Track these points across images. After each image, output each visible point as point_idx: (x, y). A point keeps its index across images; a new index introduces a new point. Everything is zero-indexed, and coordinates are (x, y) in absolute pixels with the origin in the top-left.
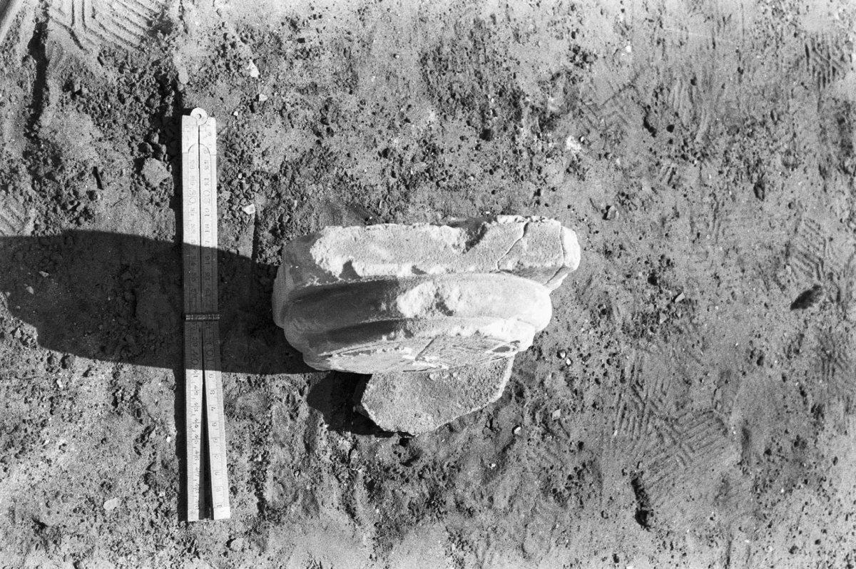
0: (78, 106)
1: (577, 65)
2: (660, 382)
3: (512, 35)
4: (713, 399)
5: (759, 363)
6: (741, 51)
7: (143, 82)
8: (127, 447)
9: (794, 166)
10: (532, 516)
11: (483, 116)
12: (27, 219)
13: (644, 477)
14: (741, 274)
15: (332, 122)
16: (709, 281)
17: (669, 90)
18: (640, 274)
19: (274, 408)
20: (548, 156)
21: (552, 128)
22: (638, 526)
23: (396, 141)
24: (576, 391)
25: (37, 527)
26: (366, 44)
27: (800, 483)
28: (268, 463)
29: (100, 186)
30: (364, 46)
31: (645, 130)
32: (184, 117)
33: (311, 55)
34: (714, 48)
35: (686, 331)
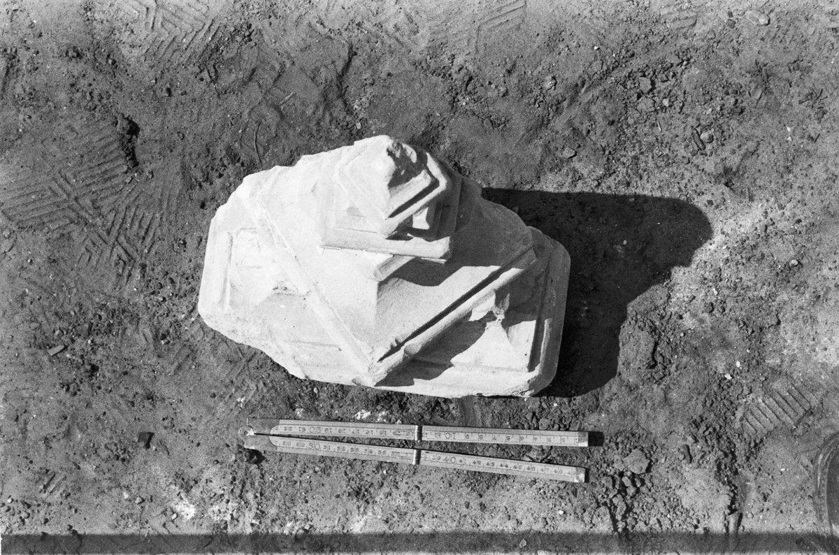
12: (741, 420)
22: (136, 121)
25: (730, 184)
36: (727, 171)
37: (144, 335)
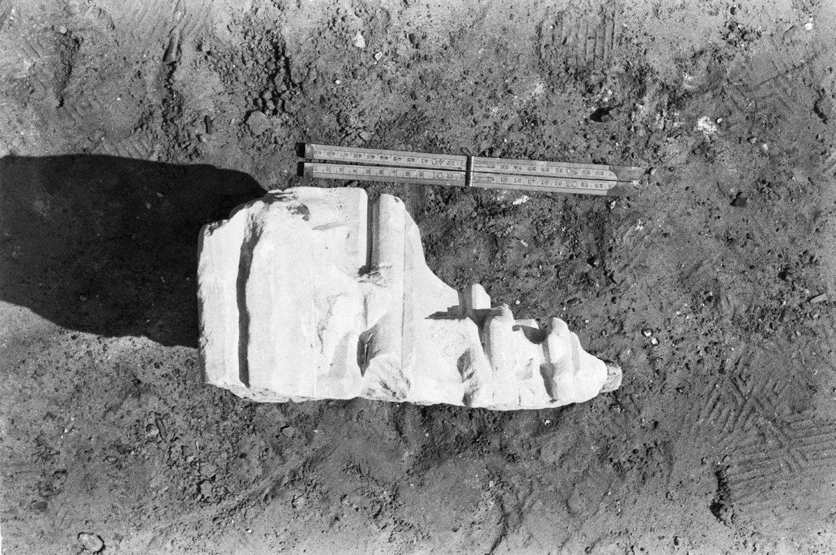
3: (651, 12)
12: (152, 152)
13: (728, 471)
21: (680, 107)
23: (495, 110)
24: (657, 371)
31: (815, 115)
36: (138, 396)
37: (729, 303)
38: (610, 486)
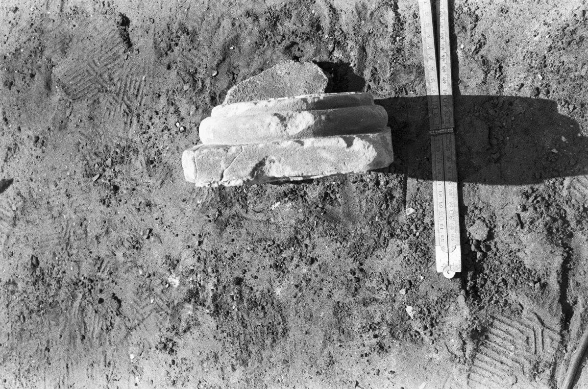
0: (535, 274)
1: (171, 340)
2: (112, 117)
4: (72, 109)
5: (38, 138)
6: (47, 365)
7: (490, 295)
8: (491, 38)
9: (8, 283)
10: (204, 16)
11: (241, 295)
12: (569, 188)
14: (50, 200)
15: (352, 280)
16: (74, 192)
17: (102, 329)
18: (125, 192)
19: (388, 75)
20: (192, 270)
21: (190, 291)
22: (127, 16)
23: (305, 271)
24: (172, 104)
26: (328, 339)
27: (9, 56)
28: (392, 37)
29: (518, 215)
30: (330, 338)
31: (120, 298)
32: (459, 271)
33: (368, 327)
34: (67, 365)
35: (91, 155)
38: (187, 16)
